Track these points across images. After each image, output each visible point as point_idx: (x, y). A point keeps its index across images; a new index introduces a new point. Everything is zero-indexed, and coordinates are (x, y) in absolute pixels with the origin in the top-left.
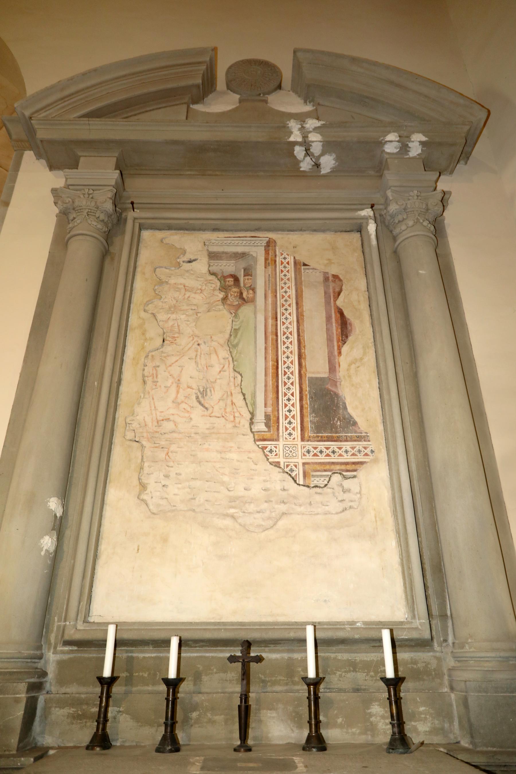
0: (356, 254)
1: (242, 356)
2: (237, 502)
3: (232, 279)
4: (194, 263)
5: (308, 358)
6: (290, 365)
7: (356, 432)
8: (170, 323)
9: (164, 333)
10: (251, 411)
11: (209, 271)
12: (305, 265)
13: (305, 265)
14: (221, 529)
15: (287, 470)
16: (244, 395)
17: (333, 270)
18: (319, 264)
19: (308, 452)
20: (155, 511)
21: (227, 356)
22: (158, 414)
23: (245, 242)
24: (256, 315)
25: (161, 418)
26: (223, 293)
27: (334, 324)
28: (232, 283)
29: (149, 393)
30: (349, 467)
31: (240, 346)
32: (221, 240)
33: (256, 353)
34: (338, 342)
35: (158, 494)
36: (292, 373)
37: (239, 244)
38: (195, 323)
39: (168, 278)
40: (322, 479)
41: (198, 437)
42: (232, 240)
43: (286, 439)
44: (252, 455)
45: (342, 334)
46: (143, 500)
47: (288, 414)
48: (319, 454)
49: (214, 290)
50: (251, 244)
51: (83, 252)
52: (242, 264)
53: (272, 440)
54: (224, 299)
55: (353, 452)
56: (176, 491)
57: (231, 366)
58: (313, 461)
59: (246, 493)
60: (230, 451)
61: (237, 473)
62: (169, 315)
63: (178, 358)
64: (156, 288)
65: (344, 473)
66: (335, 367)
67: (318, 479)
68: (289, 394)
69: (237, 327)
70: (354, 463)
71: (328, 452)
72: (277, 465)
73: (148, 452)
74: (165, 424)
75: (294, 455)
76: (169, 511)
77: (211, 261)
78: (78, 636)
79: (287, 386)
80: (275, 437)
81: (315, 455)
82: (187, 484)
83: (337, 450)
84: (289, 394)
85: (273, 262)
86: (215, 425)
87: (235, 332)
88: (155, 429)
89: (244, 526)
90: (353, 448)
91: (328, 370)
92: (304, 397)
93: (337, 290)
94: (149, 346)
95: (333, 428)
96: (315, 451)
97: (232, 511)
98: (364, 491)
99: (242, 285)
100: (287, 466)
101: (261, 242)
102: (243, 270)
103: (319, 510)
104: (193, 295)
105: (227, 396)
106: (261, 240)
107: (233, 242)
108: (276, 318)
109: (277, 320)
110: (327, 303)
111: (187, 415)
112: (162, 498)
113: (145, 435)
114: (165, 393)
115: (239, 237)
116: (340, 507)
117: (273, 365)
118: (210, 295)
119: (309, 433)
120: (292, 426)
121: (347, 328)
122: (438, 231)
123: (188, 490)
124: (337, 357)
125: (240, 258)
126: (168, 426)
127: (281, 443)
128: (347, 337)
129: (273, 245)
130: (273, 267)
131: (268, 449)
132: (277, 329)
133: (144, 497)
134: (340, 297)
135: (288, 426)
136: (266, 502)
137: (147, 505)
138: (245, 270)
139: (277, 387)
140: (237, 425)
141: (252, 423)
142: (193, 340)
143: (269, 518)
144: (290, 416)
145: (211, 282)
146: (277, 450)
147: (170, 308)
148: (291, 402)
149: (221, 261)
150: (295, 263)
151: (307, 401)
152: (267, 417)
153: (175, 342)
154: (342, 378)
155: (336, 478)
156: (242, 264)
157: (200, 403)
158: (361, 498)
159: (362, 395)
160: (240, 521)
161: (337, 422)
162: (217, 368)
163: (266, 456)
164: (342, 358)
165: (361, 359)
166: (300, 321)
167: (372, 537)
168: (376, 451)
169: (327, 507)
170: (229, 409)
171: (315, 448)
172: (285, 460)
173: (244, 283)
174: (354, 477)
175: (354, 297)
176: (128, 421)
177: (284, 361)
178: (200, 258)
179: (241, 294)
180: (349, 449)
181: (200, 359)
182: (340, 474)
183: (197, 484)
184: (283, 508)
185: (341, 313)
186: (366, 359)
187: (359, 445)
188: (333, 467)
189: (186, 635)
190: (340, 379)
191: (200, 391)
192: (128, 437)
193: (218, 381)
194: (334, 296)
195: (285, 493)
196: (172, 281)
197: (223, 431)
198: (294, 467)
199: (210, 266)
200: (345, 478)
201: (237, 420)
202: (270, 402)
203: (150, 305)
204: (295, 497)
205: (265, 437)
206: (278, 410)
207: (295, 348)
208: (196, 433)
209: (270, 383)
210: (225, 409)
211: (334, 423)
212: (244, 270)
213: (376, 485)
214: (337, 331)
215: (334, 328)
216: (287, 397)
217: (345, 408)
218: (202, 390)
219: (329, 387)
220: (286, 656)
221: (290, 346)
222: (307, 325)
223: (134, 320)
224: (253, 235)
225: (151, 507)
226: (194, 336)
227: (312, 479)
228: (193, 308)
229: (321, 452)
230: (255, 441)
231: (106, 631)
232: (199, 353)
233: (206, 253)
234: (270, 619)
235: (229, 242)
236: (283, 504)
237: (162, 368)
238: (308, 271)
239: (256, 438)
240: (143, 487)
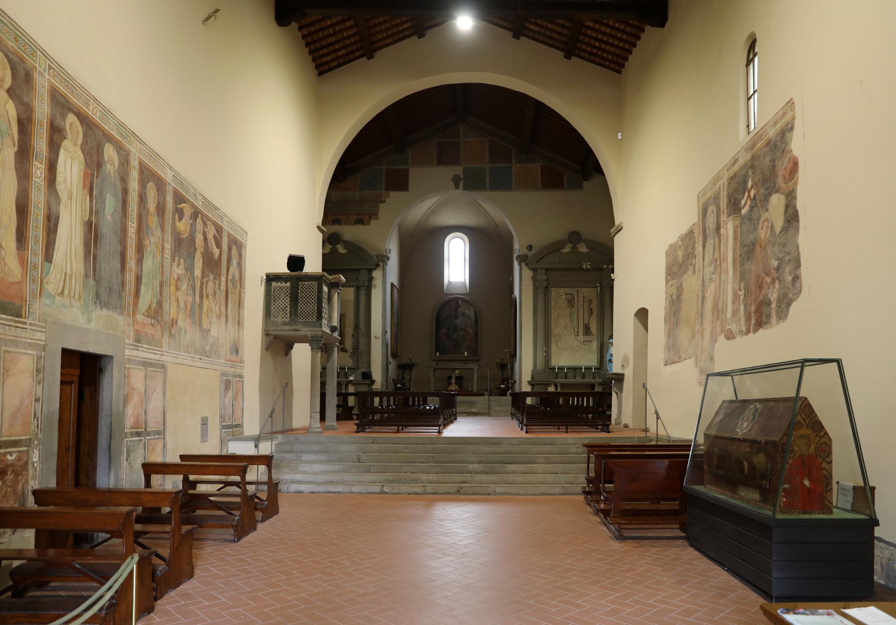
159: (594, 328)
213: (595, 345)
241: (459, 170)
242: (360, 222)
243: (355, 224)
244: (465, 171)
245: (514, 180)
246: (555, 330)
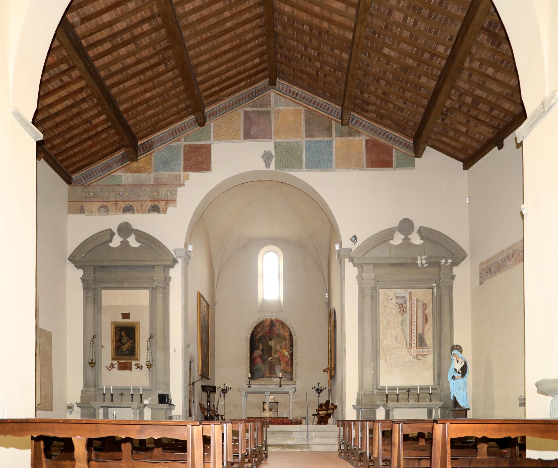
17: (425, 302)
24: (407, 316)
87: (402, 321)
122: (451, 288)
126: (390, 346)
159: (429, 339)
207: (415, 325)
213: (430, 358)
222: (418, 319)
240: (386, 360)
241: (269, 146)
242: (155, 209)
243: (149, 212)
244: (277, 146)
245: (334, 157)
246: (385, 341)
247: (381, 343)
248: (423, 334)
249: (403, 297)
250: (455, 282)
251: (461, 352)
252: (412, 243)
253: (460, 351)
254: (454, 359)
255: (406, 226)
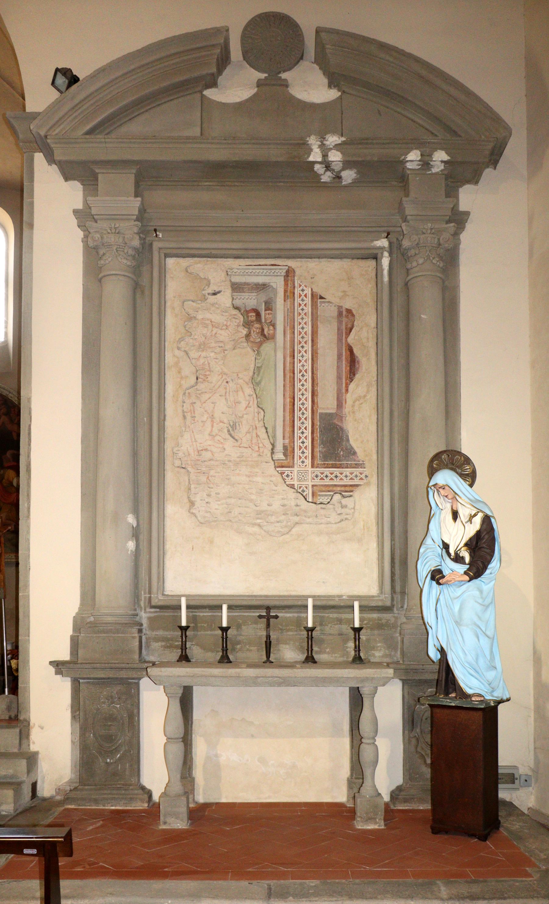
0: (370, 286)
1: (265, 393)
2: (263, 515)
3: (254, 314)
4: (219, 295)
5: (320, 395)
6: (305, 401)
7: (355, 461)
8: (202, 361)
9: (197, 371)
10: (272, 441)
11: (233, 304)
12: (321, 298)
13: (321, 298)
14: (251, 534)
15: (300, 490)
16: (266, 428)
17: (348, 304)
18: (333, 296)
19: (317, 476)
20: (202, 521)
21: (252, 393)
22: (198, 445)
23: (265, 271)
24: (275, 352)
25: (201, 449)
26: (247, 330)
27: (344, 362)
28: (254, 318)
29: (189, 427)
30: (347, 489)
31: (263, 384)
32: (243, 269)
33: (276, 390)
34: (346, 380)
35: (203, 509)
36: (306, 409)
37: (260, 274)
38: (223, 361)
39: (196, 313)
40: (326, 498)
41: (231, 464)
42: (253, 269)
43: (300, 466)
44: (273, 479)
45: (350, 372)
46: (192, 513)
47: (301, 445)
48: (325, 478)
49: (238, 326)
50: (272, 274)
51: (116, 291)
52: (263, 297)
53: (289, 467)
54: (248, 336)
55: (351, 476)
56: (217, 507)
57: (256, 402)
58: (320, 483)
59: (269, 508)
60: (256, 476)
61: (262, 493)
62: (200, 353)
63: (211, 395)
64: (186, 323)
65: (343, 493)
66: (342, 403)
67: (323, 498)
68: (303, 428)
69: (259, 365)
70: (351, 486)
71: (332, 476)
72: (292, 486)
73: (193, 477)
74: (204, 453)
75: (306, 478)
76: (213, 521)
77: (234, 294)
78: (160, 603)
79: (301, 421)
80: (291, 464)
81: (322, 479)
82: (224, 501)
83: (339, 475)
84: (303, 428)
85: (292, 295)
86: (244, 454)
87: (258, 369)
88: (197, 458)
89: (267, 532)
90: (351, 474)
91: (336, 407)
92: (315, 430)
93: (349, 326)
94: (186, 384)
95: (337, 457)
96: (322, 476)
97: (258, 521)
98: (357, 507)
99: (263, 320)
100: (300, 487)
101: (281, 271)
102: (264, 304)
103: (323, 521)
104: (220, 332)
105: (253, 430)
106: (280, 269)
107: (254, 271)
108: (294, 356)
109: (294, 358)
110: (340, 340)
111: (221, 446)
112: (207, 512)
113: (189, 462)
114: (202, 427)
115: (260, 265)
116: (338, 518)
117: (290, 402)
118: (234, 332)
119: (318, 461)
120: (305, 455)
121: (355, 366)
122: (449, 260)
123: (226, 506)
124: (344, 394)
125: (260, 290)
126: (207, 455)
127: (296, 469)
128: (354, 375)
129: (292, 274)
130: (292, 300)
131: (285, 474)
132: (294, 367)
133: (193, 511)
134: (351, 333)
135: (301, 455)
136: (284, 514)
137: (196, 517)
138: (266, 303)
139: (294, 421)
140: (261, 454)
141: (273, 453)
142: (222, 377)
143: (286, 526)
144: (303, 447)
145: (235, 317)
146: (293, 475)
147: (200, 345)
148: (304, 435)
149: (243, 294)
150: (312, 295)
151: (317, 435)
152: (285, 448)
153: (207, 379)
154: (347, 413)
155: (337, 497)
156: (263, 297)
157: (231, 435)
158: (354, 513)
159: (362, 430)
160: (264, 528)
161: (340, 452)
162: (244, 404)
163: (284, 479)
164: (349, 395)
165: (365, 396)
166: (315, 359)
167: (360, 540)
168: (369, 476)
169: (328, 519)
170: (254, 441)
171: (322, 473)
172: (299, 483)
173: (265, 317)
174: (351, 496)
175: (364, 334)
176: (174, 451)
177: (300, 398)
178: (223, 290)
179: (263, 330)
180: (348, 474)
181: (229, 396)
182: (340, 494)
183: (233, 501)
184: (296, 519)
185: (351, 350)
186: (368, 397)
187: (357, 471)
188: (335, 488)
189: (231, 603)
190: (345, 414)
191: (230, 425)
192: (176, 465)
193: (245, 416)
194: (346, 332)
195: (298, 508)
196: (200, 317)
197: (250, 459)
198: (305, 489)
199: (233, 299)
200: (344, 497)
201: (261, 450)
202: (287, 435)
203: (182, 343)
204: (305, 511)
205: (283, 465)
206: (294, 442)
207: (309, 385)
208: (229, 461)
209: (288, 418)
210: (251, 441)
211: (338, 453)
212: (265, 304)
213: (366, 503)
214: (346, 369)
215: (344, 365)
216: (301, 430)
217: (348, 440)
218: (232, 424)
219: (336, 421)
220: (296, 615)
221: (305, 383)
222: (320, 362)
223: (169, 358)
224: (273, 263)
225: (199, 518)
226: (223, 373)
227: (319, 498)
228: (220, 345)
229: (327, 476)
230: (275, 467)
231: (180, 601)
232: (228, 391)
233: (229, 284)
234: (286, 593)
235: (250, 271)
236: (296, 517)
237: (198, 404)
238: (323, 305)
239: (276, 464)
240: (192, 503)
246: (187, 435)
247: (169, 446)
248: (339, 414)
249: (262, 287)
250: (466, 238)
251: (471, 478)
252: (292, 97)
253: (463, 476)
254: (442, 506)
255: (274, 41)
